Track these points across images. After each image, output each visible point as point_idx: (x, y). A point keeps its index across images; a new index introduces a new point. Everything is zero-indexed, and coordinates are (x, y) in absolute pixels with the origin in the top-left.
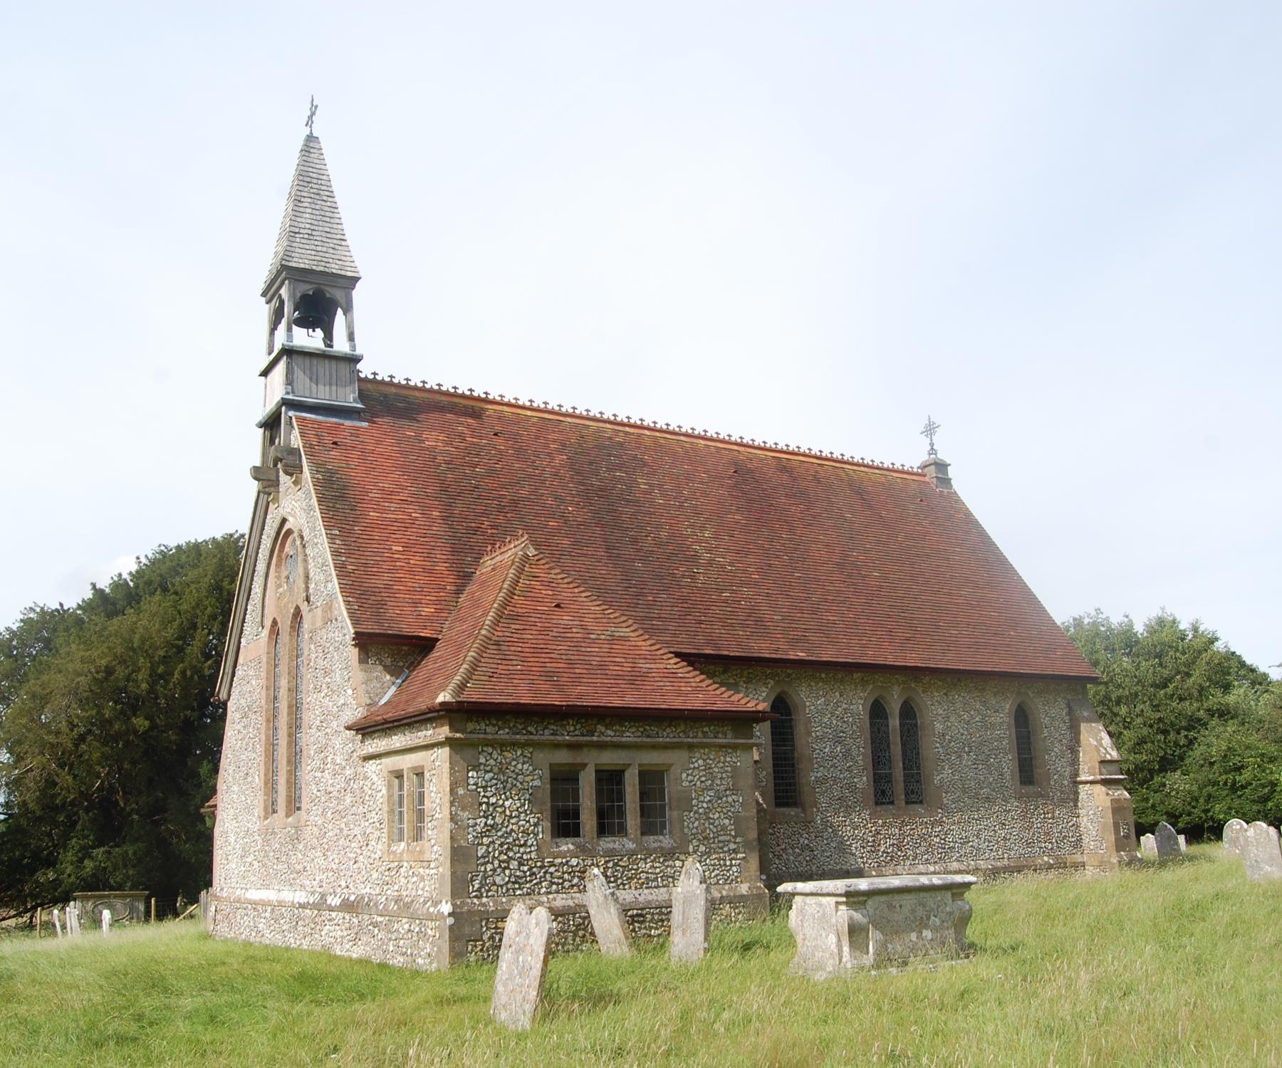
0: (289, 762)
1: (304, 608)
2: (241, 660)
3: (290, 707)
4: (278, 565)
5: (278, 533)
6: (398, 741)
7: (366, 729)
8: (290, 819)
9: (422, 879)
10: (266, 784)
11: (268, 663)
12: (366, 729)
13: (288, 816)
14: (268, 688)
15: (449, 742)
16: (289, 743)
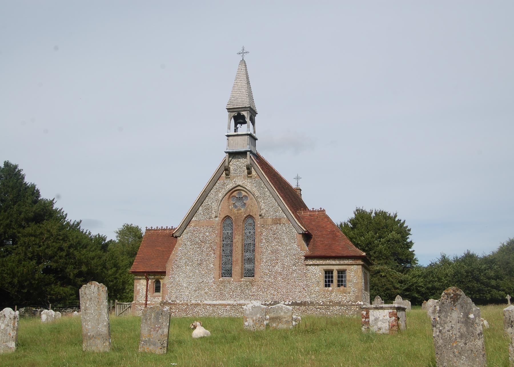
0: (242, 262)
1: (257, 217)
2: (192, 224)
3: (242, 245)
4: (229, 198)
5: (232, 189)
6: (333, 262)
7: (307, 258)
8: (242, 279)
9: (345, 296)
10: (220, 267)
11: (221, 229)
12: (307, 258)
13: (241, 278)
14: (220, 237)
15: (362, 265)
16: (242, 256)
